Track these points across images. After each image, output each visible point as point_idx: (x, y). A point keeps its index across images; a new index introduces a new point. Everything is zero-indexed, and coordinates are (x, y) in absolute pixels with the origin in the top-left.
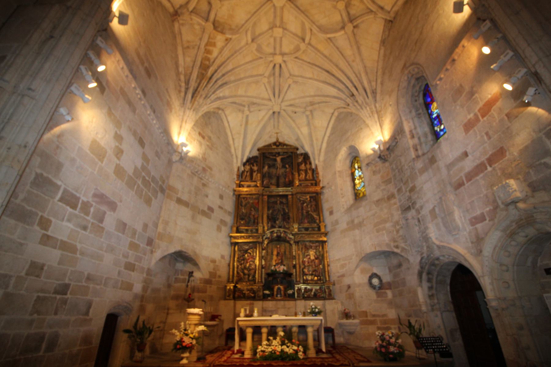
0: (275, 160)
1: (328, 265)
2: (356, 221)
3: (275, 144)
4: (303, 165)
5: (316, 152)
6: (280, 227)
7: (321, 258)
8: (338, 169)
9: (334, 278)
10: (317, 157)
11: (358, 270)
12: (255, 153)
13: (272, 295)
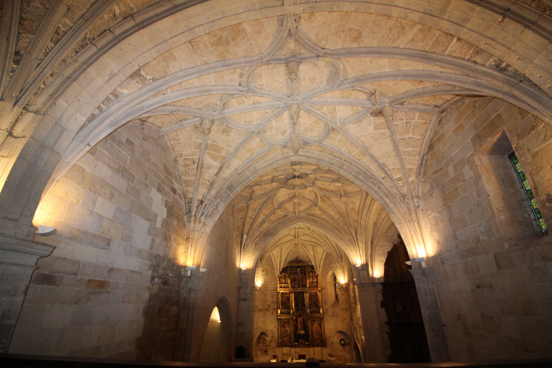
0: (297, 270)
1: (324, 330)
2: (335, 314)
3: (296, 261)
4: (311, 273)
5: (318, 266)
6: (301, 310)
7: (320, 325)
8: (328, 281)
9: (326, 336)
10: (318, 269)
11: (336, 336)
12: (286, 266)
13: (299, 345)
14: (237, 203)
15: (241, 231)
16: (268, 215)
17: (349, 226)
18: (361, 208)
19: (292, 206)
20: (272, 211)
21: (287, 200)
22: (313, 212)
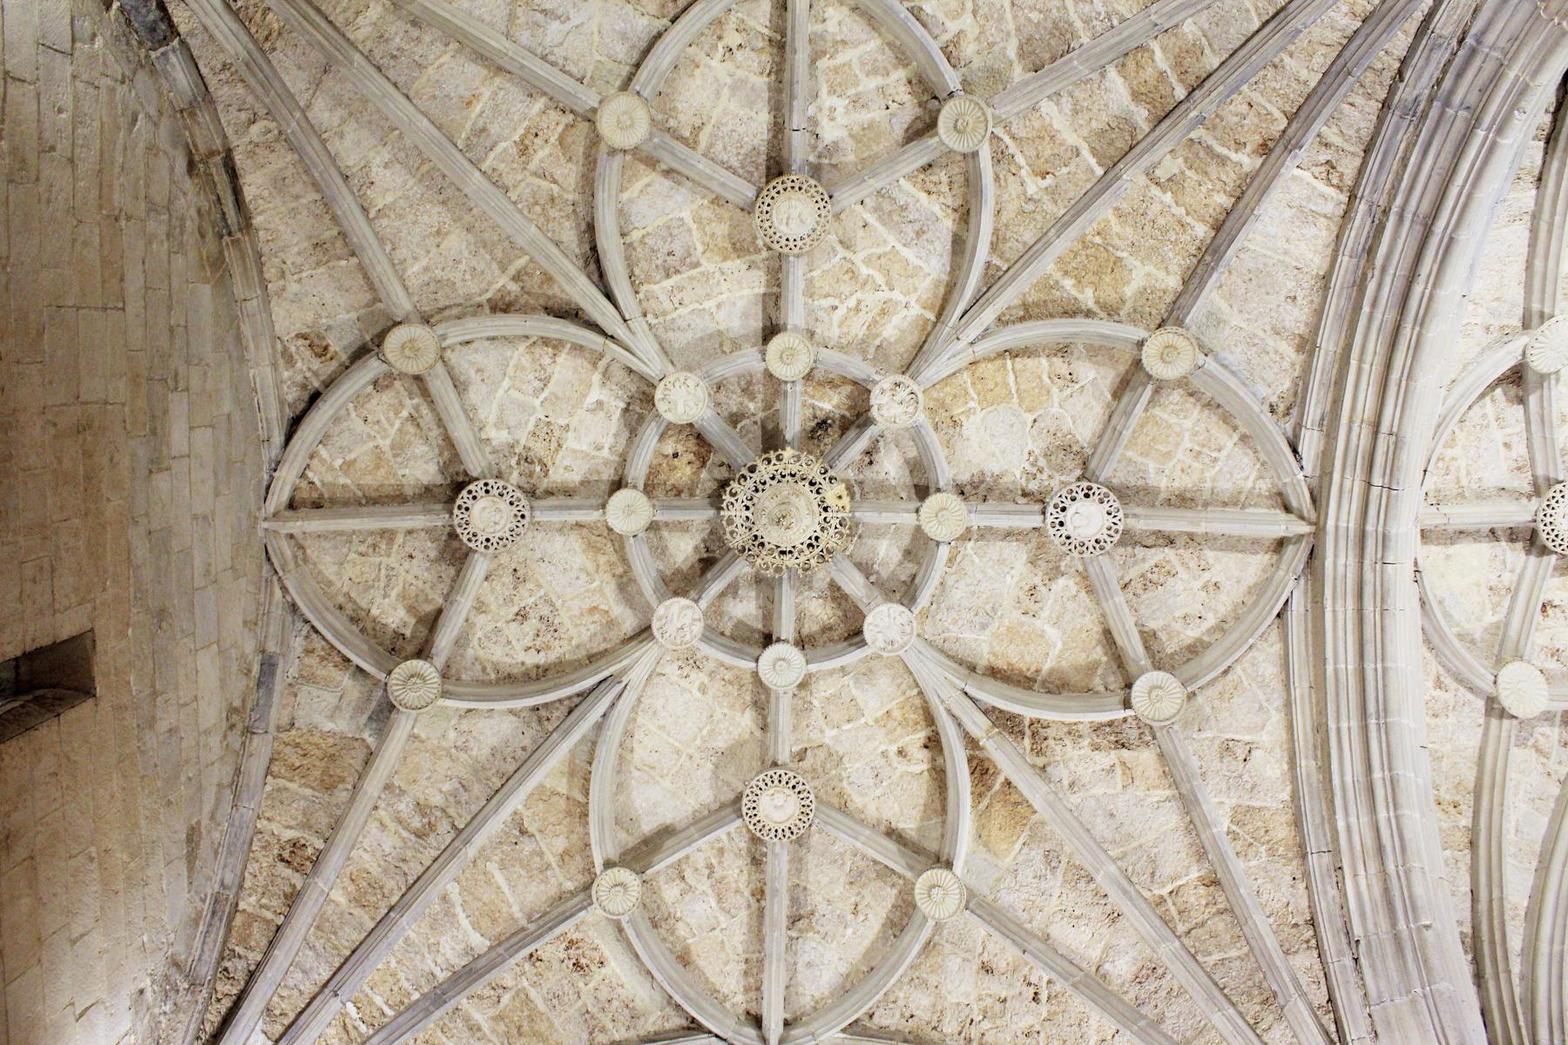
14: (308, 678)
15: (239, 968)
16: (523, 929)
17: (1253, 1008)
18: (1307, 764)
19: (736, 931)
20: (560, 898)
21: (696, 821)
22: (920, 1003)
